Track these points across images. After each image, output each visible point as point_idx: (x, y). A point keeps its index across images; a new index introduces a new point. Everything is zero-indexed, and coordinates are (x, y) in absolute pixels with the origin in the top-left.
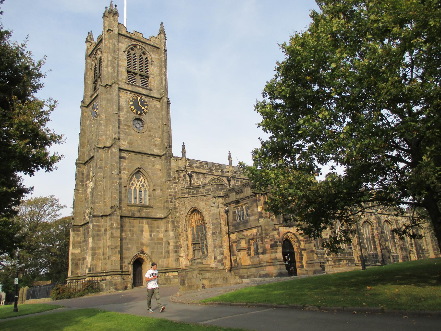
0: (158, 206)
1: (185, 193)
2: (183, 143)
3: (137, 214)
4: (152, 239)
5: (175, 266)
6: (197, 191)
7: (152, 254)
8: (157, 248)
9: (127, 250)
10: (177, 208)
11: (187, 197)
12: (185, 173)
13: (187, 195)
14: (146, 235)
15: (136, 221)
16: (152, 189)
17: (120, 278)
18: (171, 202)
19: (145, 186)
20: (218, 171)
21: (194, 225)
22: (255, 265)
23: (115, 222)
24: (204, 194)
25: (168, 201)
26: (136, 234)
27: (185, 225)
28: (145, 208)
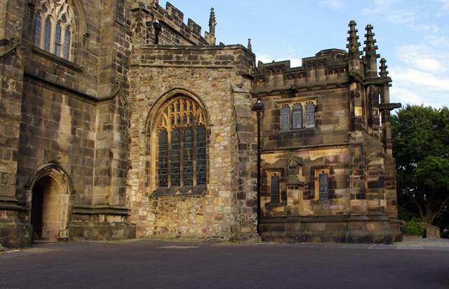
0: (91, 71)
1: (154, 58)
3: (51, 77)
4: (74, 141)
5: (117, 203)
6: (190, 58)
7: (72, 172)
8: (84, 160)
9: (25, 155)
10: (127, 86)
11: (161, 67)
12: (149, 19)
13: (157, 62)
14: (65, 128)
15: (48, 93)
16: (82, 32)
17: (13, 218)
18: (120, 70)
19: (69, 20)
20: (196, 38)
21: (169, 128)
22: (325, 217)
23: (11, 81)
24: (214, 65)
25: (115, 65)
26: (46, 122)
27: (147, 123)
28: (66, 69)
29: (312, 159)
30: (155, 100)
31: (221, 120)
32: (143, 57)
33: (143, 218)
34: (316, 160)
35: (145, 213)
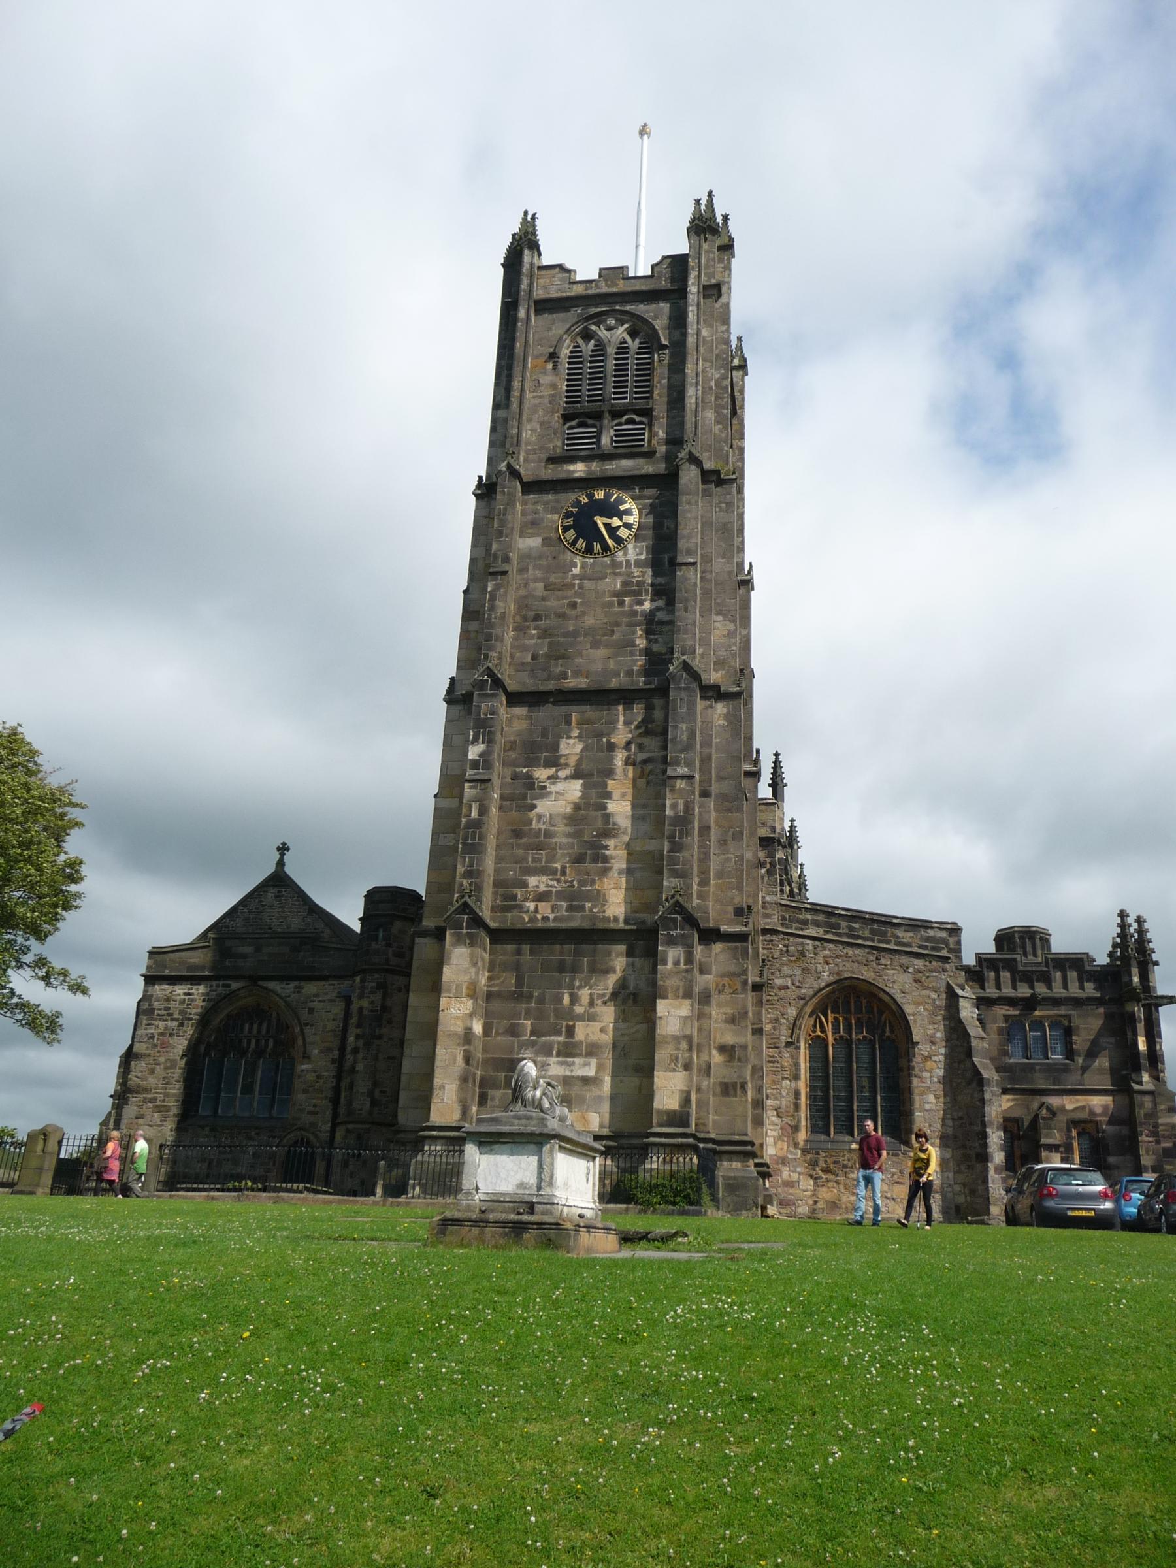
1: (805, 922)
2: (777, 755)
6: (872, 932)
13: (811, 931)
27: (794, 1027)
29: (1069, 1107)
30: (811, 992)
31: (932, 1036)
32: (784, 918)
33: (789, 1184)
34: (1076, 1109)
35: (795, 1176)
